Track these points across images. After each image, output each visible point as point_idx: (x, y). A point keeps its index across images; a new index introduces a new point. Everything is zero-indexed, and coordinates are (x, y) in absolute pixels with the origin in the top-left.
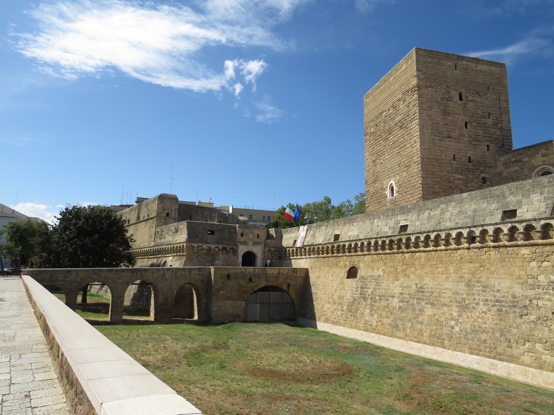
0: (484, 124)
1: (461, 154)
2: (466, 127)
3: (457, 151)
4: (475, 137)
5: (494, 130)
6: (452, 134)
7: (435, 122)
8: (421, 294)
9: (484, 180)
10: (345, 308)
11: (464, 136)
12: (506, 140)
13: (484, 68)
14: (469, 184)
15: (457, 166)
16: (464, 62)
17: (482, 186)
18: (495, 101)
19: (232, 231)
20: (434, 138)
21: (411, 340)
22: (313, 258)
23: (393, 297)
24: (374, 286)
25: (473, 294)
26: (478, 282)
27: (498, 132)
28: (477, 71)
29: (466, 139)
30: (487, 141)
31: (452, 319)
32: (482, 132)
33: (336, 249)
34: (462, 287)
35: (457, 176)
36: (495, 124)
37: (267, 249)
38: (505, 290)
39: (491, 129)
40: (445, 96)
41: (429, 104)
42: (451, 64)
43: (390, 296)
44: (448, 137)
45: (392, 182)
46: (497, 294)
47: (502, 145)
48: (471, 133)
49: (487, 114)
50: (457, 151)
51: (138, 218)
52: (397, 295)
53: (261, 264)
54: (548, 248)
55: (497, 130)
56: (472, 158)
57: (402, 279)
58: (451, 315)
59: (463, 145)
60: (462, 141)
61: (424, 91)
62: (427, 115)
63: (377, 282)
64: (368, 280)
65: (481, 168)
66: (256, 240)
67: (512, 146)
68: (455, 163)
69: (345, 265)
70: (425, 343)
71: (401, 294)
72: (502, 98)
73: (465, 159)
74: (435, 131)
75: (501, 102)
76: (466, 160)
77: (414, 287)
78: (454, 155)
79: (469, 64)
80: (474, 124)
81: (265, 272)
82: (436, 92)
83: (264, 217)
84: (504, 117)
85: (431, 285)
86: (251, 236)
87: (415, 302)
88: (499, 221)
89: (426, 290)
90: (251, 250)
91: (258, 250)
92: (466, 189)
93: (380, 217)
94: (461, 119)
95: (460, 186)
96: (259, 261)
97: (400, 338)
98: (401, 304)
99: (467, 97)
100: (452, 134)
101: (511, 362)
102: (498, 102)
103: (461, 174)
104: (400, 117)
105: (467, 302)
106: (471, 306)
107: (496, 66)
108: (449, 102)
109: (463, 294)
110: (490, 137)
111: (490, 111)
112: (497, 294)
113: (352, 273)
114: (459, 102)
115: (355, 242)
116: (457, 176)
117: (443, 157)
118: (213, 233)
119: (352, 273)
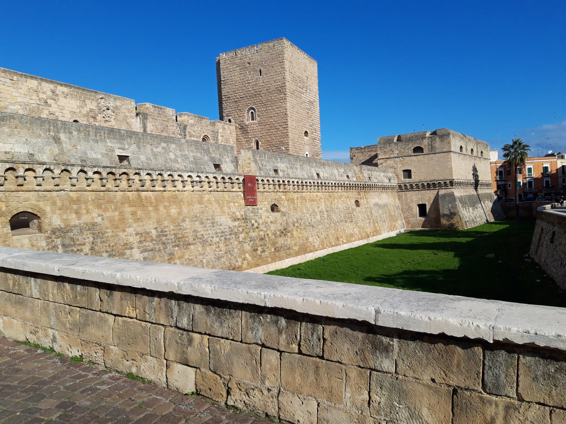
8: (164, 238)
23: (132, 248)
24: (91, 239)
25: (207, 230)
26: (207, 220)
31: (200, 254)
38: (224, 224)
43: (126, 249)
46: (221, 227)
52: (135, 245)
54: (235, 194)
58: (198, 250)
63: (93, 233)
64: (75, 231)
71: (140, 242)
77: (154, 232)
85: (172, 227)
87: (162, 248)
89: (168, 233)
93: (71, 133)
98: (146, 254)
105: (205, 237)
106: (209, 240)
109: (200, 232)
112: (221, 227)
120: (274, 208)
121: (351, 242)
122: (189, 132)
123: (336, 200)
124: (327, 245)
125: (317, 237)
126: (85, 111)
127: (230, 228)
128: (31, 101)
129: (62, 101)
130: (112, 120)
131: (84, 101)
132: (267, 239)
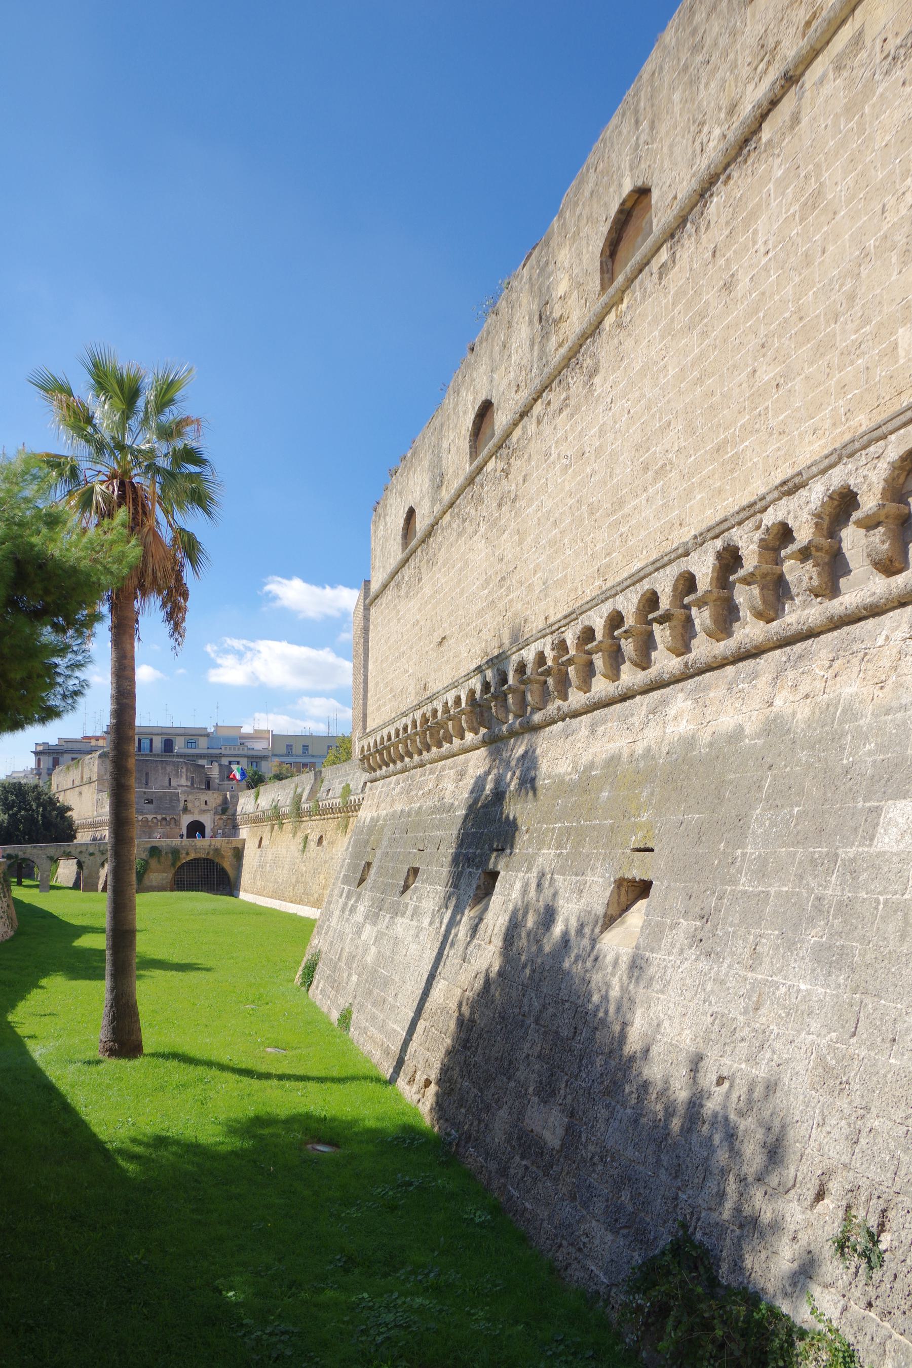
19: (174, 798)
51: (82, 778)
66: (204, 807)
86: (197, 803)
91: (207, 820)
96: (208, 831)
118: (150, 802)
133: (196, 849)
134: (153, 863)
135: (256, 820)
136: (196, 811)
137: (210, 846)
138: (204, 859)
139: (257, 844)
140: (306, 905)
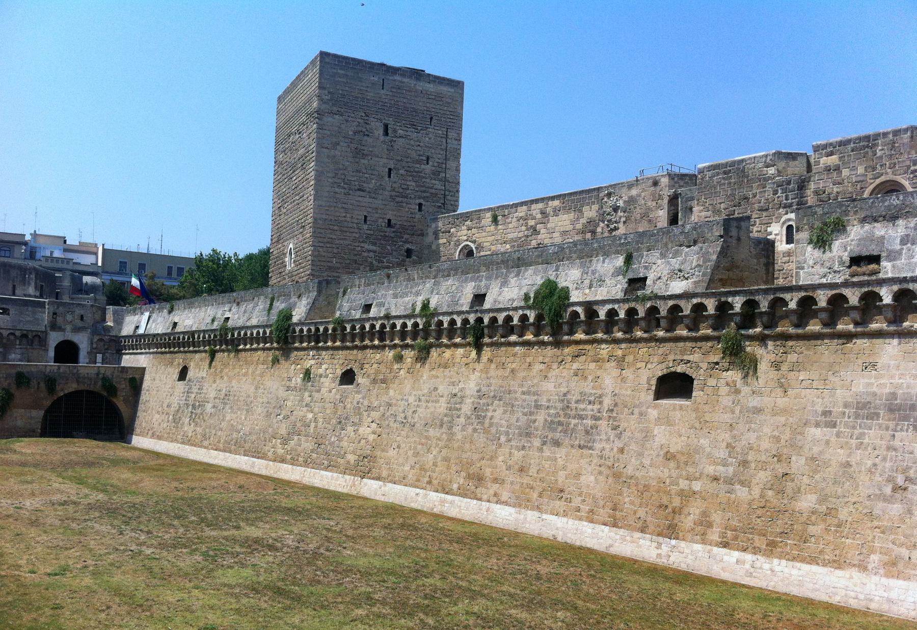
0: (418, 172)
1: (377, 215)
2: (389, 177)
3: (370, 210)
4: (401, 190)
5: (433, 182)
6: (365, 185)
7: (341, 166)
9: (409, 253)
10: (171, 417)
11: (384, 189)
12: (449, 198)
13: (431, 87)
14: (384, 258)
15: (369, 232)
16: (397, 78)
17: (404, 261)
18: (439, 139)
20: (337, 189)
21: (212, 449)
22: (153, 353)
27: (438, 185)
28: (416, 91)
29: (387, 193)
30: (419, 198)
32: (414, 184)
33: (171, 343)
34: (252, 389)
35: (367, 246)
36: (436, 174)
37: (96, 338)
39: (428, 180)
40: (360, 129)
41: (334, 140)
42: (376, 79)
44: (359, 190)
45: (291, 246)
47: (444, 204)
48: (394, 185)
49: (425, 158)
50: (370, 210)
53: (87, 360)
55: (437, 182)
56: (393, 222)
57: (218, 382)
59: (380, 202)
60: (381, 197)
61: (328, 119)
62: (328, 157)
65: (406, 236)
66: (79, 323)
67: (457, 206)
68: (366, 227)
69: (179, 364)
70: (220, 450)
71: (215, 398)
72: (452, 134)
73: (383, 223)
74: (339, 181)
75: (449, 141)
76: (383, 224)
78: (366, 217)
79: (406, 80)
80: (402, 172)
81: (75, 371)
82: (347, 121)
83: (170, 268)
84: (451, 164)
86: (69, 317)
88: (466, 308)
90: (61, 339)
91: (82, 341)
92: (380, 265)
94: (382, 164)
95: (370, 260)
97: (205, 448)
99: (395, 131)
100: (365, 185)
101: (262, 458)
102: (444, 140)
103: (374, 244)
104: (302, 151)
107: (448, 84)
108: (366, 138)
110: (424, 192)
111: (429, 154)
113: (183, 374)
114: (382, 138)
115: (401, 321)
116: (367, 246)
117: (348, 219)
119: (183, 374)
120: (348, 377)
121: (538, 508)
122: (816, 193)
123: (538, 367)
124: (429, 482)
125: (410, 453)
126: (579, 226)
127: (278, 398)
128: (520, 235)
129: (553, 222)
130: (621, 225)
131: (581, 211)
132: (313, 425)
133: (78, 378)
134: (19, 395)
135: (171, 343)
136: (69, 327)
137: (98, 374)
138: (88, 391)
139: (176, 376)
140: (326, 469)
